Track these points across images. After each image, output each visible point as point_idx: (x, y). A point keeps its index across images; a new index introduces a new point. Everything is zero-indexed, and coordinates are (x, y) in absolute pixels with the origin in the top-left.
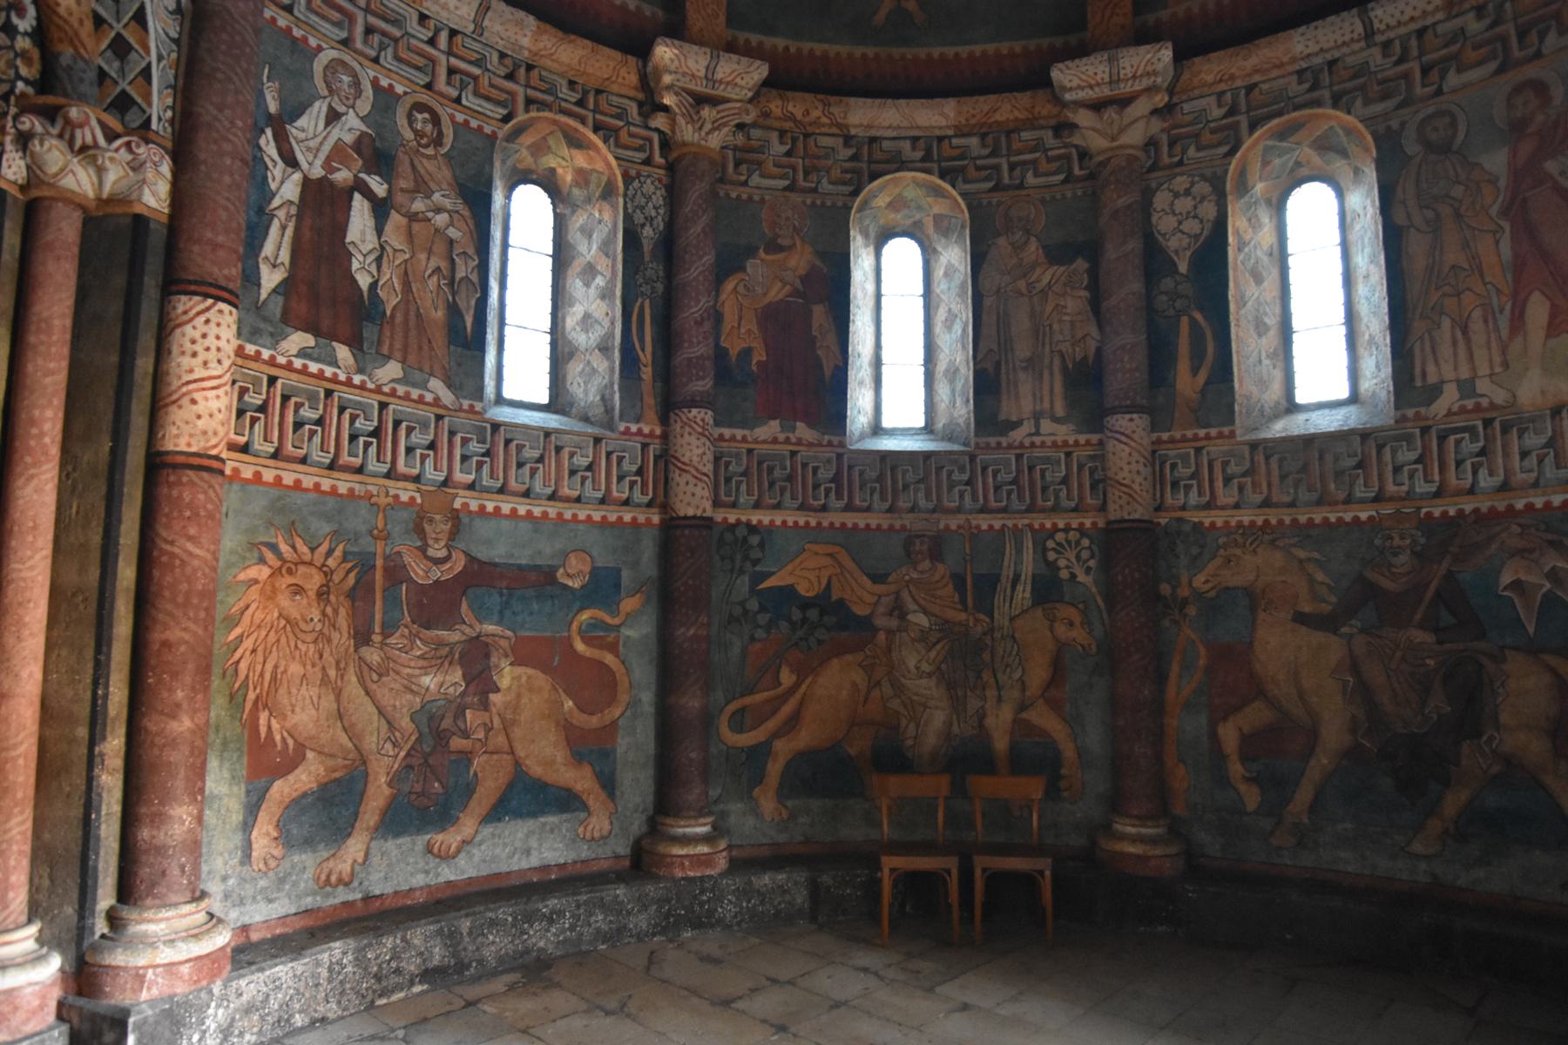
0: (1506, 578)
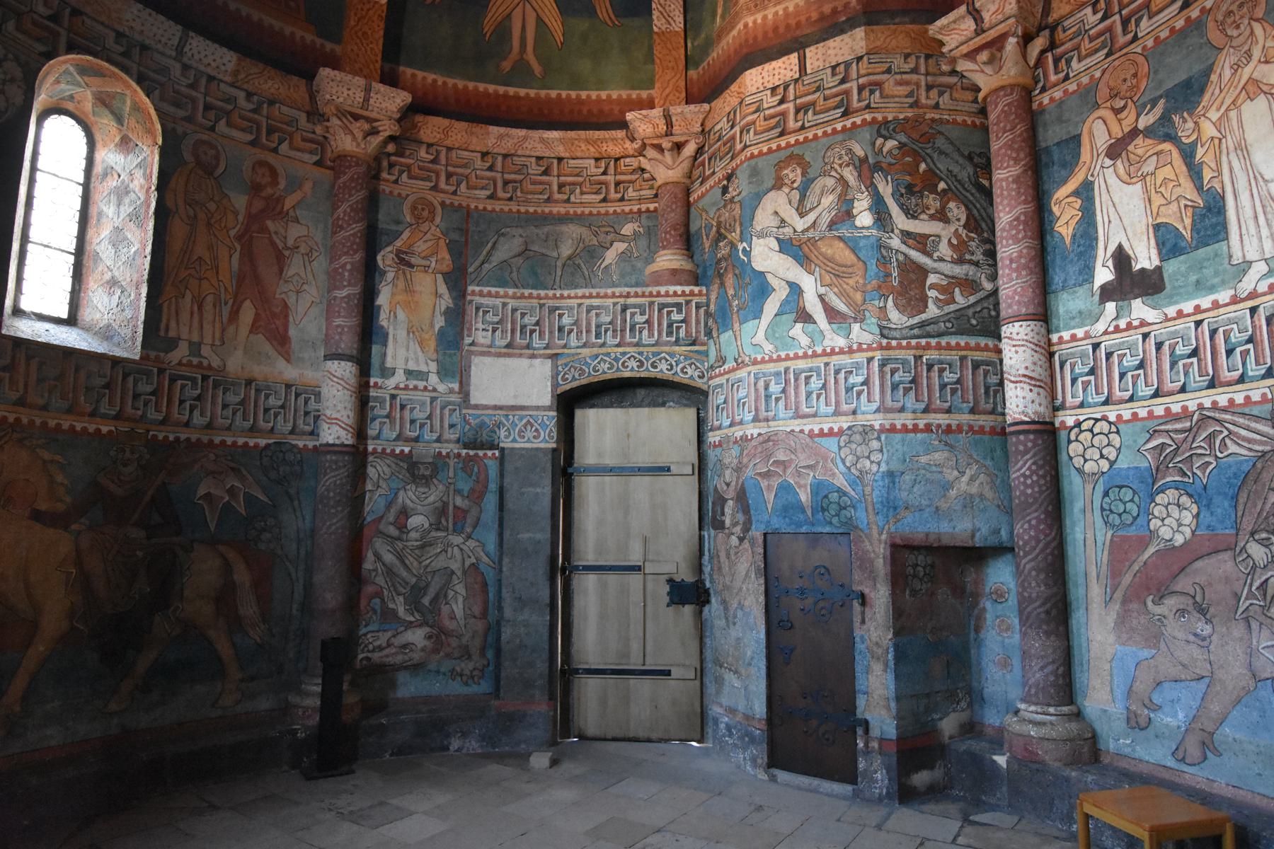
0: (202, 491)
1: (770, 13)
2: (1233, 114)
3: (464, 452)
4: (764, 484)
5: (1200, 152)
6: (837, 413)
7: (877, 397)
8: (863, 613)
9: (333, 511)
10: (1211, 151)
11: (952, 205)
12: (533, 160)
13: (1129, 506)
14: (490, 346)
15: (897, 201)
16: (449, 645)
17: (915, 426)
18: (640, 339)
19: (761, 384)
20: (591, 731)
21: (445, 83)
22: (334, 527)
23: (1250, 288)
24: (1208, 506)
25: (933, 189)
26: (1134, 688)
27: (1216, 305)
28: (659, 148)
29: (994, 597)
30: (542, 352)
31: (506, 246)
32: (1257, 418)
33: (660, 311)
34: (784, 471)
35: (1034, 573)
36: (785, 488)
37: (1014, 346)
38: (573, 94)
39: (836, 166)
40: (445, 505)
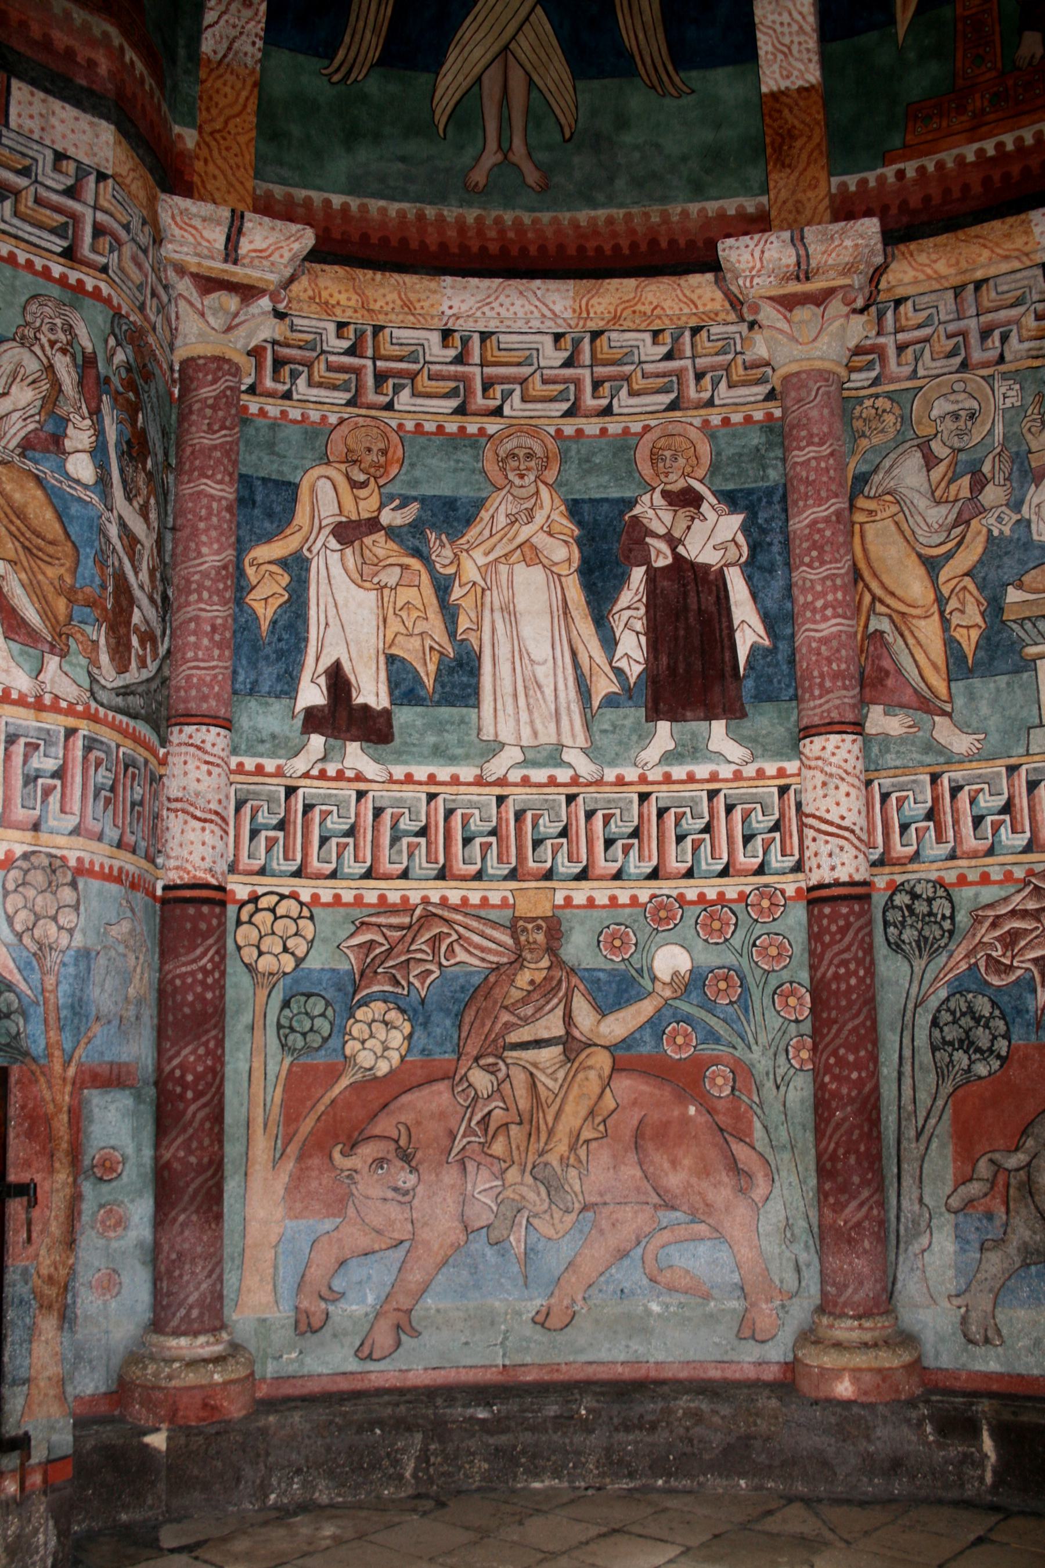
2: (503, 569)
5: (457, 593)
7: (76, 808)
8: (29, 1223)
10: (471, 597)
13: (319, 1022)
15: (120, 459)
23: (500, 773)
24: (425, 1025)
26: (307, 1278)
27: (455, 781)
29: (98, 1172)
32: (495, 924)
37: (207, 763)
39: (44, 340)
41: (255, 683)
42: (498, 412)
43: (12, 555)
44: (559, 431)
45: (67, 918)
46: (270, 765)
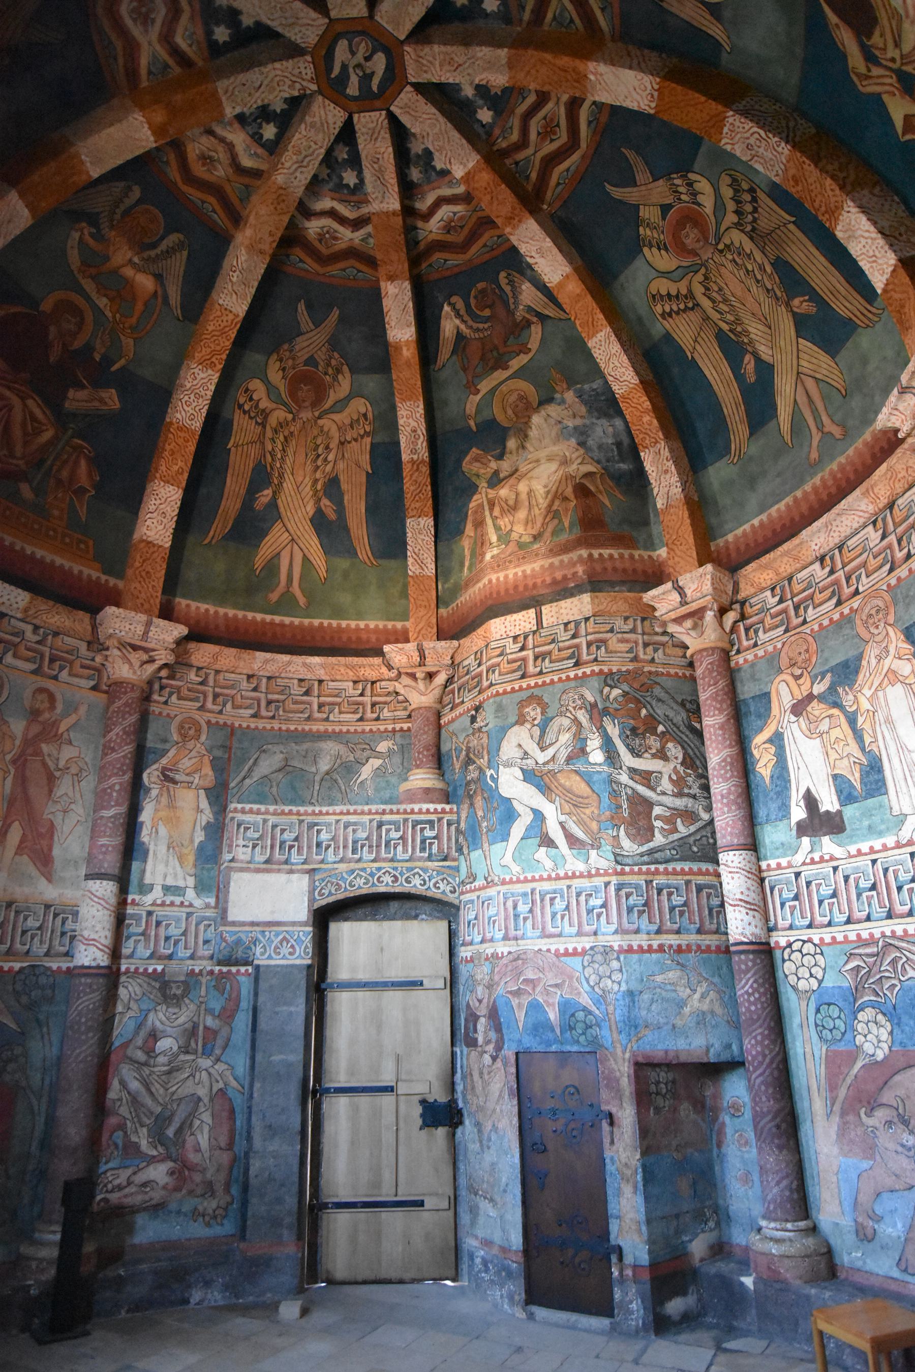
1: (511, 573)
2: (880, 694)
3: (217, 969)
4: (515, 1002)
5: (860, 720)
6: (580, 934)
8: (612, 1133)
9: (83, 1037)
10: (868, 720)
11: (670, 745)
12: (296, 682)
14: (249, 862)
15: (623, 741)
16: (192, 1181)
17: (650, 946)
18: (395, 854)
19: (510, 904)
20: (340, 1273)
21: (216, 612)
22: (83, 1055)
24: (898, 1024)
25: (653, 731)
28: (413, 676)
29: (732, 1111)
30: (300, 867)
31: (267, 763)
33: (414, 827)
34: (534, 989)
35: (763, 1088)
36: (535, 1007)
38: (334, 623)
40: (195, 1026)
41: (768, 815)
42: (857, 592)
43: (568, 811)
44: (889, 585)
45: (617, 976)
46: (784, 862)
